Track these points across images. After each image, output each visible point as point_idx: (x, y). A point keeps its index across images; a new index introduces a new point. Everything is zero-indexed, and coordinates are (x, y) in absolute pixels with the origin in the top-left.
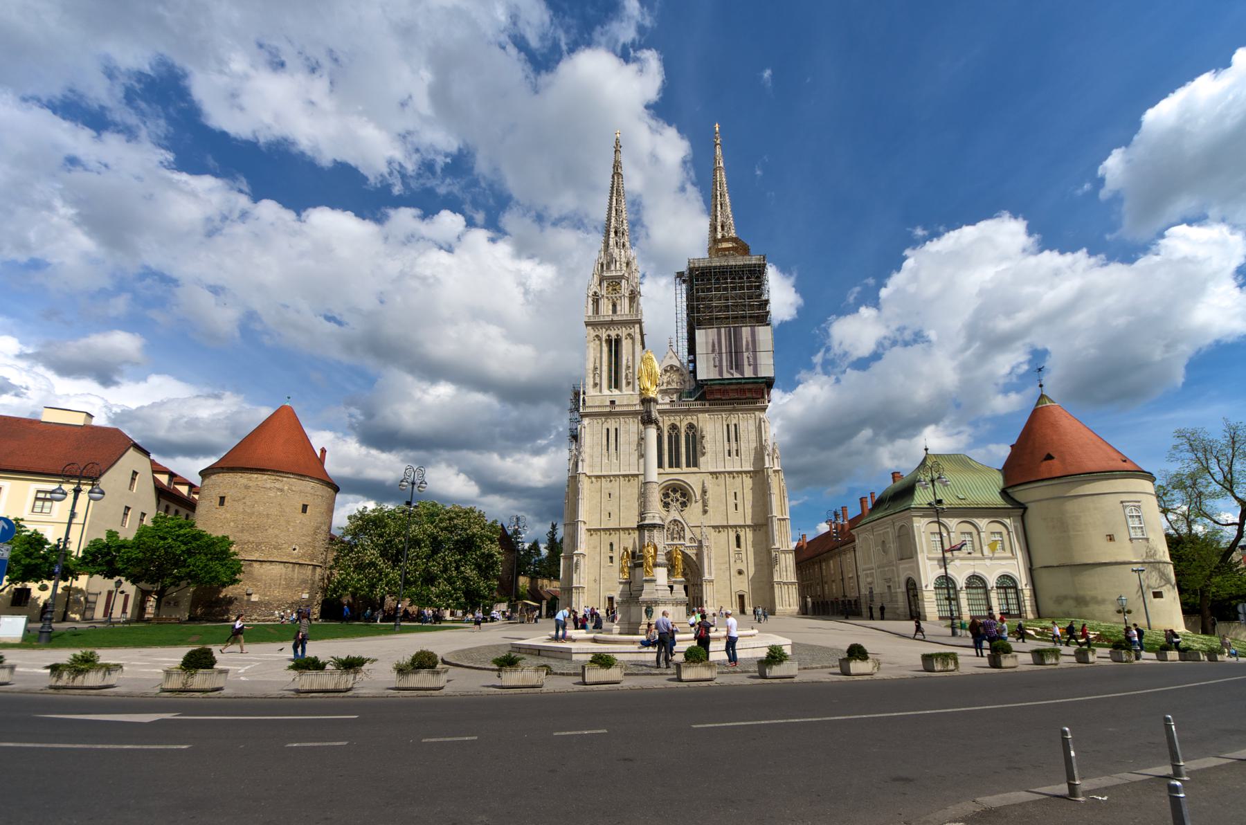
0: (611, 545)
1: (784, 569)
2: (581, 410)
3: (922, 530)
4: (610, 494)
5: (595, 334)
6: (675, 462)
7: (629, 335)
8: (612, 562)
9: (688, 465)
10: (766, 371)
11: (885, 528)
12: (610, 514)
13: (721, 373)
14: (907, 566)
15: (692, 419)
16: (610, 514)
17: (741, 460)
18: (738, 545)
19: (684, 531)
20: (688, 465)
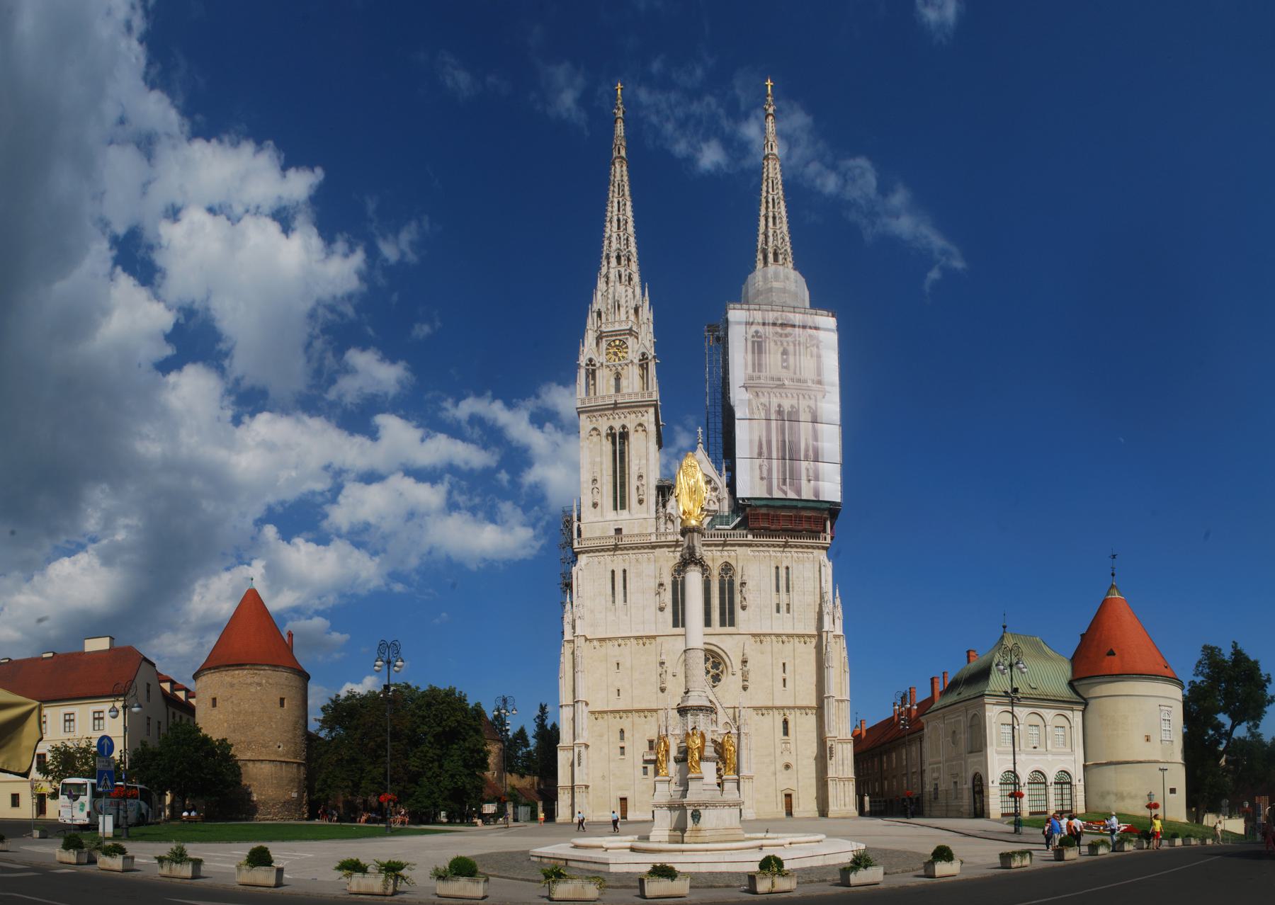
0: (622, 731)
1: (841, 762)
2: (576, 545)
3: (994, 720)
4: (618, 664)
5: (592, 427)
7: (641, 425)
8: (623, 753)
9: (723, 624)
10: (831, 489)
11: (958, 716)
13: (770, 490)
14: (975, 760)
15: (729, 557)
17: (793, 618)
18: (786, 733)
20: (723, 624)
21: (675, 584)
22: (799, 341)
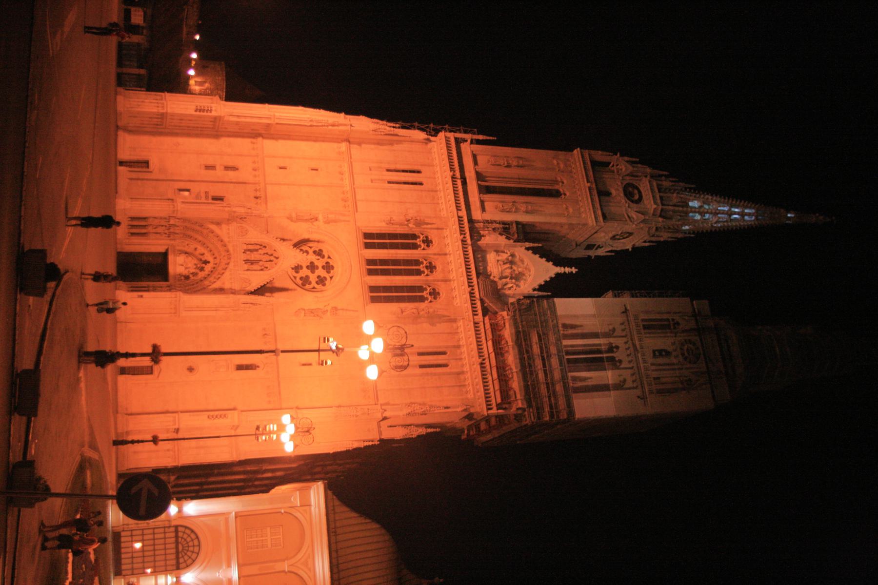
0: (234, 169)
6: (374, 267)
12: (285, 168)
16: (285, 168)
19: (262, 270)
21: (414, 236)
22: (682, 369)
